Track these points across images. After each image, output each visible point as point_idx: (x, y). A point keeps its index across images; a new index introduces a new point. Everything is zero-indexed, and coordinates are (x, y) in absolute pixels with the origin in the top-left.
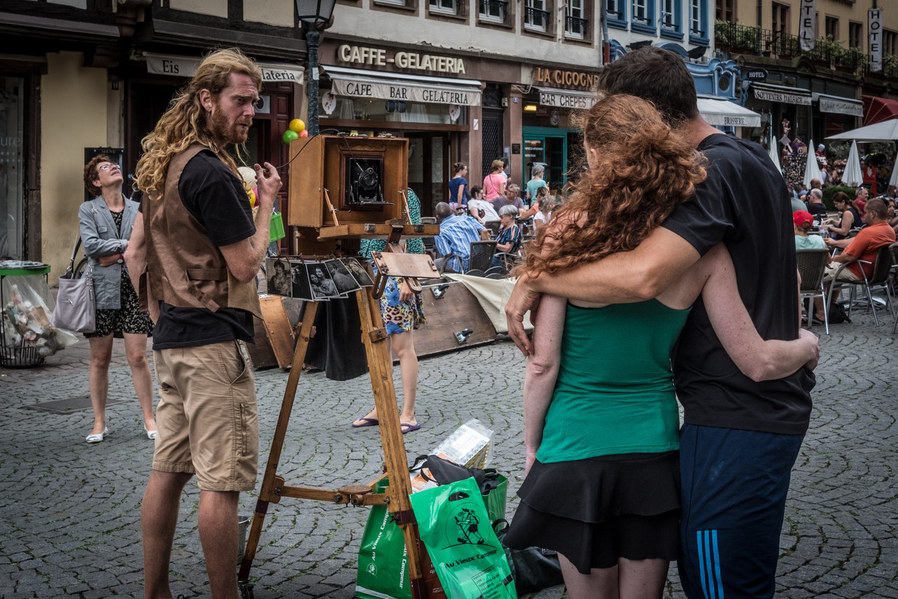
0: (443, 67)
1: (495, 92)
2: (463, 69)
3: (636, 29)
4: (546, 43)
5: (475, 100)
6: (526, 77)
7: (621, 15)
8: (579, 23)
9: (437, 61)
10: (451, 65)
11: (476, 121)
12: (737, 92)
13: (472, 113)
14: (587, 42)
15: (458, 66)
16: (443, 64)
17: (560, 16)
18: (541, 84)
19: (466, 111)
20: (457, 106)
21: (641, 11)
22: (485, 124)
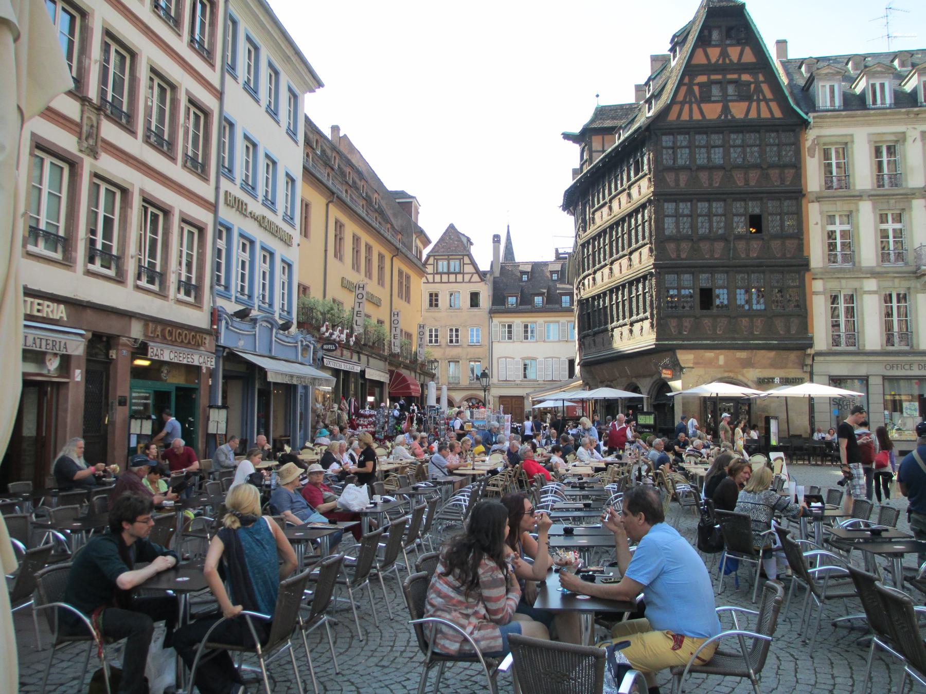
0: (39, 311)
1: (101, 343)
2: (64, 316)
3: (238, 301)
4: (159, 302)
5: (77, 347)
6: (136, 331)
7: (227, 288)
8: (191, 288)
9: (32, 303)
10: (49, 310)
11: (78, 372)
12: (314, 360)
13: (73, 363)
14: (198, 305)
15: (59, 312)
16: (40, 307)
17: (172, 279)
18: (152, 339)
19: (66, 362)
20: (55, 355)
21: (243, 287)
22: (89, 376)
